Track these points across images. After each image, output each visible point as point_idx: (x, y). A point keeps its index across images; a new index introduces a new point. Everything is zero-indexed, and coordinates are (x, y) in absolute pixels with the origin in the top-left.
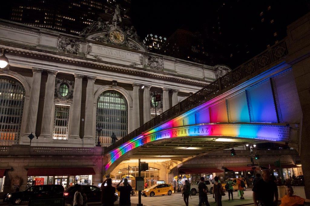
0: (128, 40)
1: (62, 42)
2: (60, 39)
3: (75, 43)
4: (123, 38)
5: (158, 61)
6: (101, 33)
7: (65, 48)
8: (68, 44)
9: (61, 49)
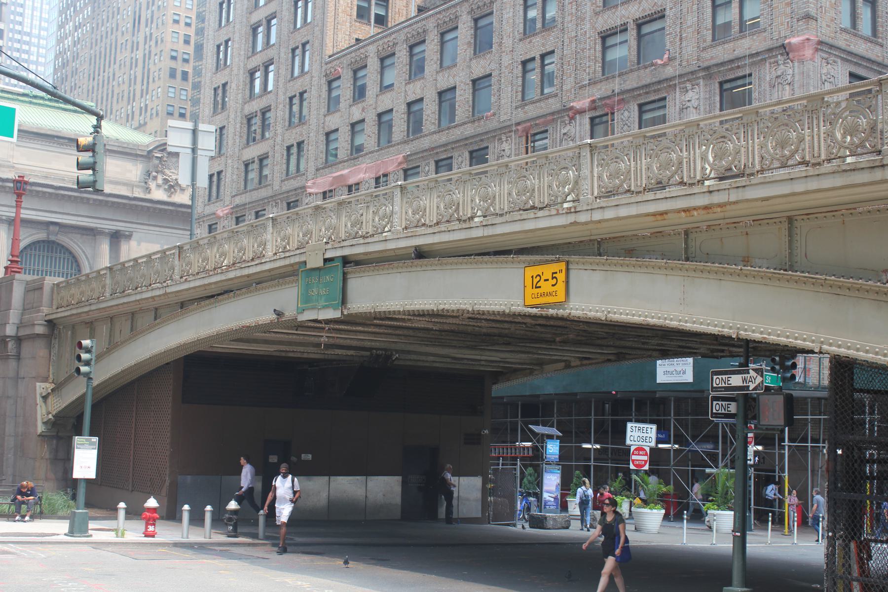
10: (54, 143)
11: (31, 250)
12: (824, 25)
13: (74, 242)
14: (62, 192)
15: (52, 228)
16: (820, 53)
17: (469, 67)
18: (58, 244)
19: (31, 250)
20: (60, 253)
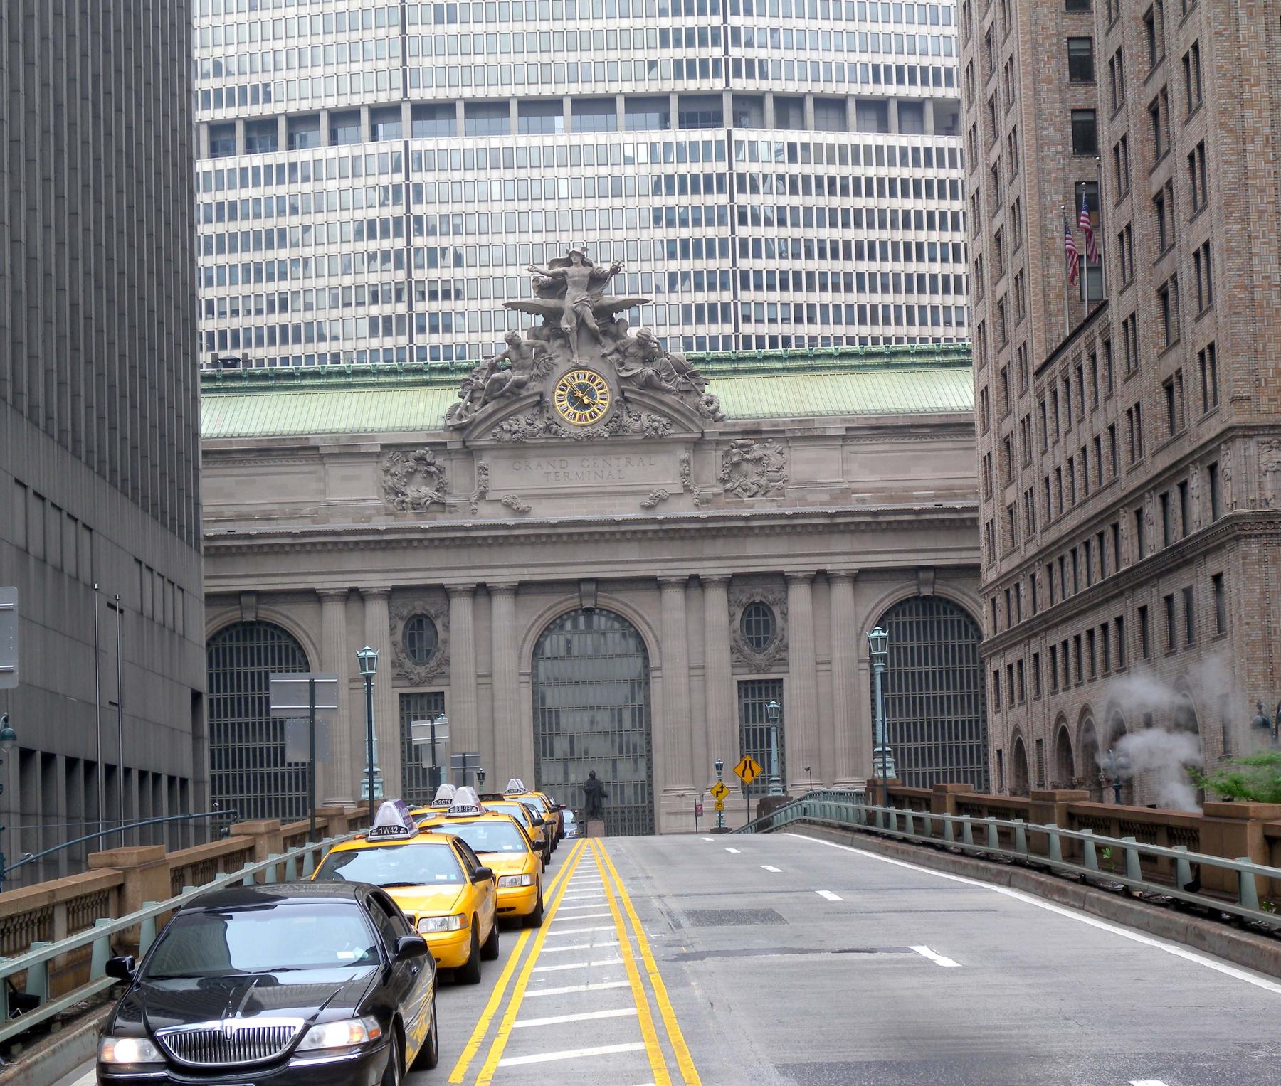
0: (626, 400)
1: (392, 471)
2: (386, 463)
3: (433, 464)
4: (608, 396)
5: (767, 452)
6: (517, 406)
7: (403, 494)
8: (410, 475)
9: (392, 497)
10: (910, 437)
11: (897, 615)
12: (1265, 400)
13: (964, 594)
14: (928, 517)
15: (922, 575)
16: (1255, 439)
17: (1105, 410)
18: (941, 599)
19: (897, 615)
20: (945, 613)
